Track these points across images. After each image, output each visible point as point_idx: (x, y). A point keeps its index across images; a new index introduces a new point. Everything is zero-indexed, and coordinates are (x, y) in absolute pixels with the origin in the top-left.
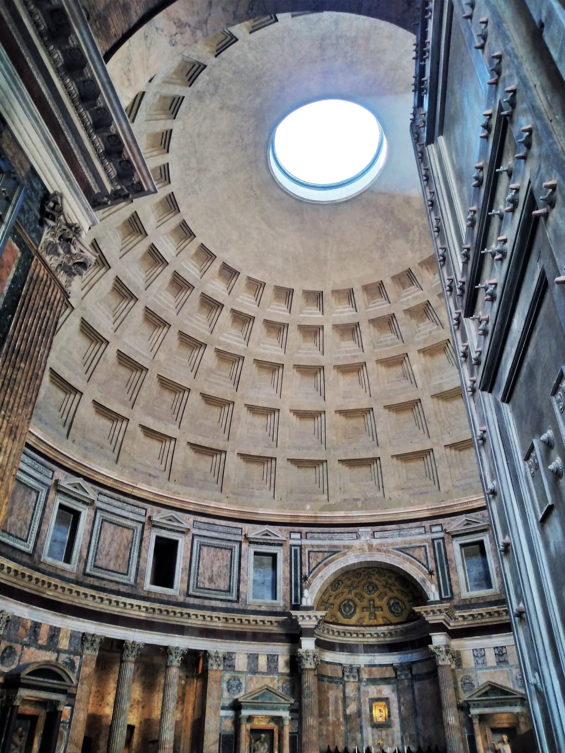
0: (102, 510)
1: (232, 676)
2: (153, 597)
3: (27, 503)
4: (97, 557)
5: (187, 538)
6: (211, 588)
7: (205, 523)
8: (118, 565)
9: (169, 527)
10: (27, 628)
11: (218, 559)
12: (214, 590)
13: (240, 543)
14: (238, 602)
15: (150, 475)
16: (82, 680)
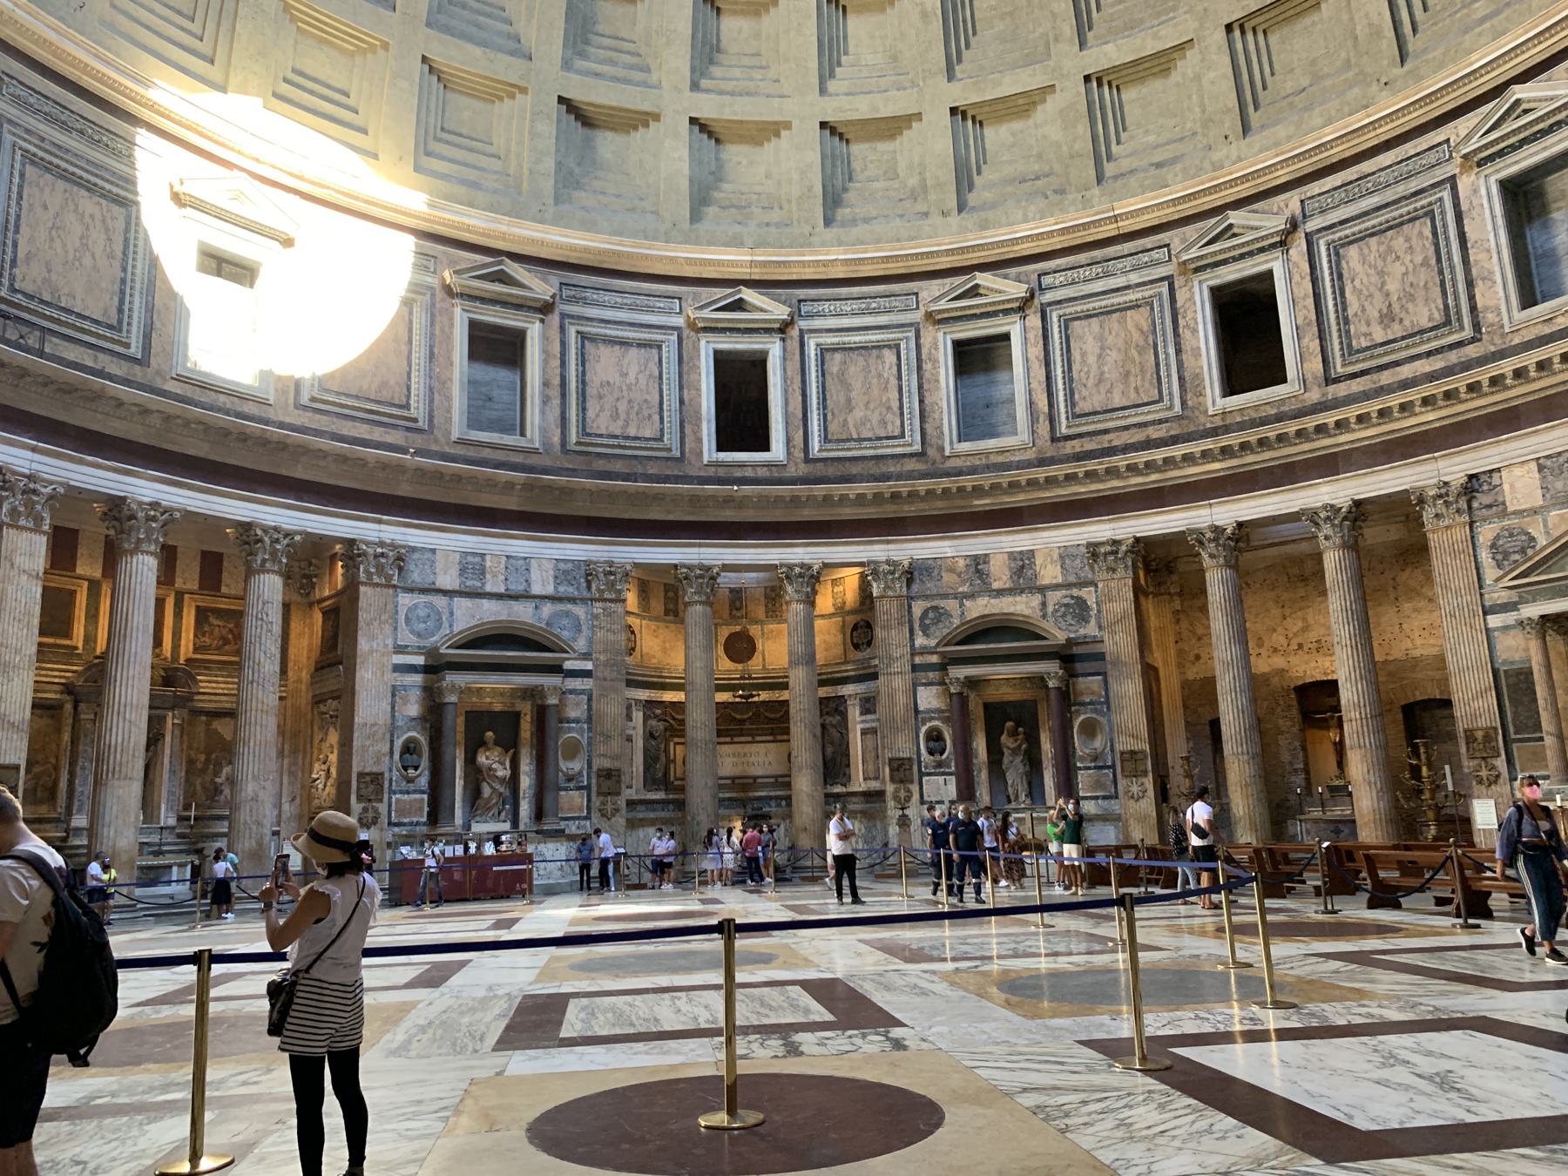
0: (1059, 302)
1: (1503, 529)
2: (1239, 419)
3: (880, 375)
4: (1076, 396)
5: (1291, 252)
6: (1391, 337)
7: (1335, 189)
8: (1132, 390)
9: (1236, 253)
10: (958, 570)
11: (1398, 258)
12: (1403, 338)
13: (1453, 177)
14: (1480, 340)
15: (1159, 165)
16: (1111, 625)
